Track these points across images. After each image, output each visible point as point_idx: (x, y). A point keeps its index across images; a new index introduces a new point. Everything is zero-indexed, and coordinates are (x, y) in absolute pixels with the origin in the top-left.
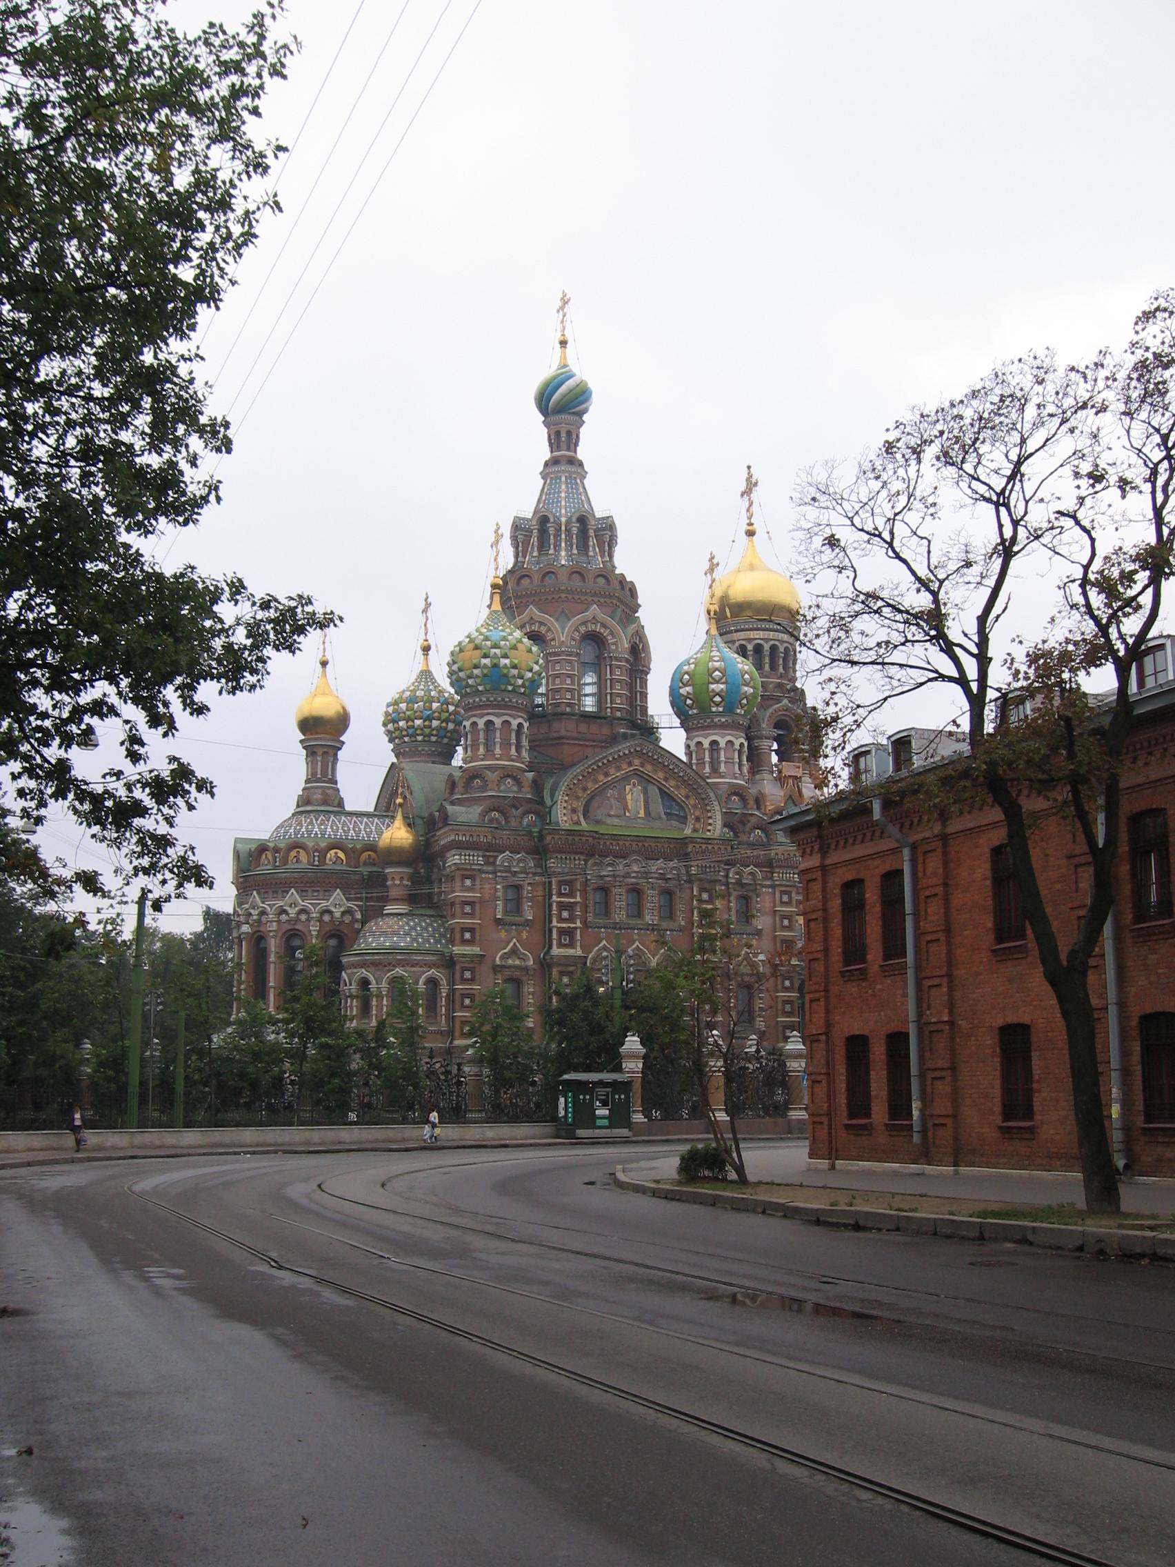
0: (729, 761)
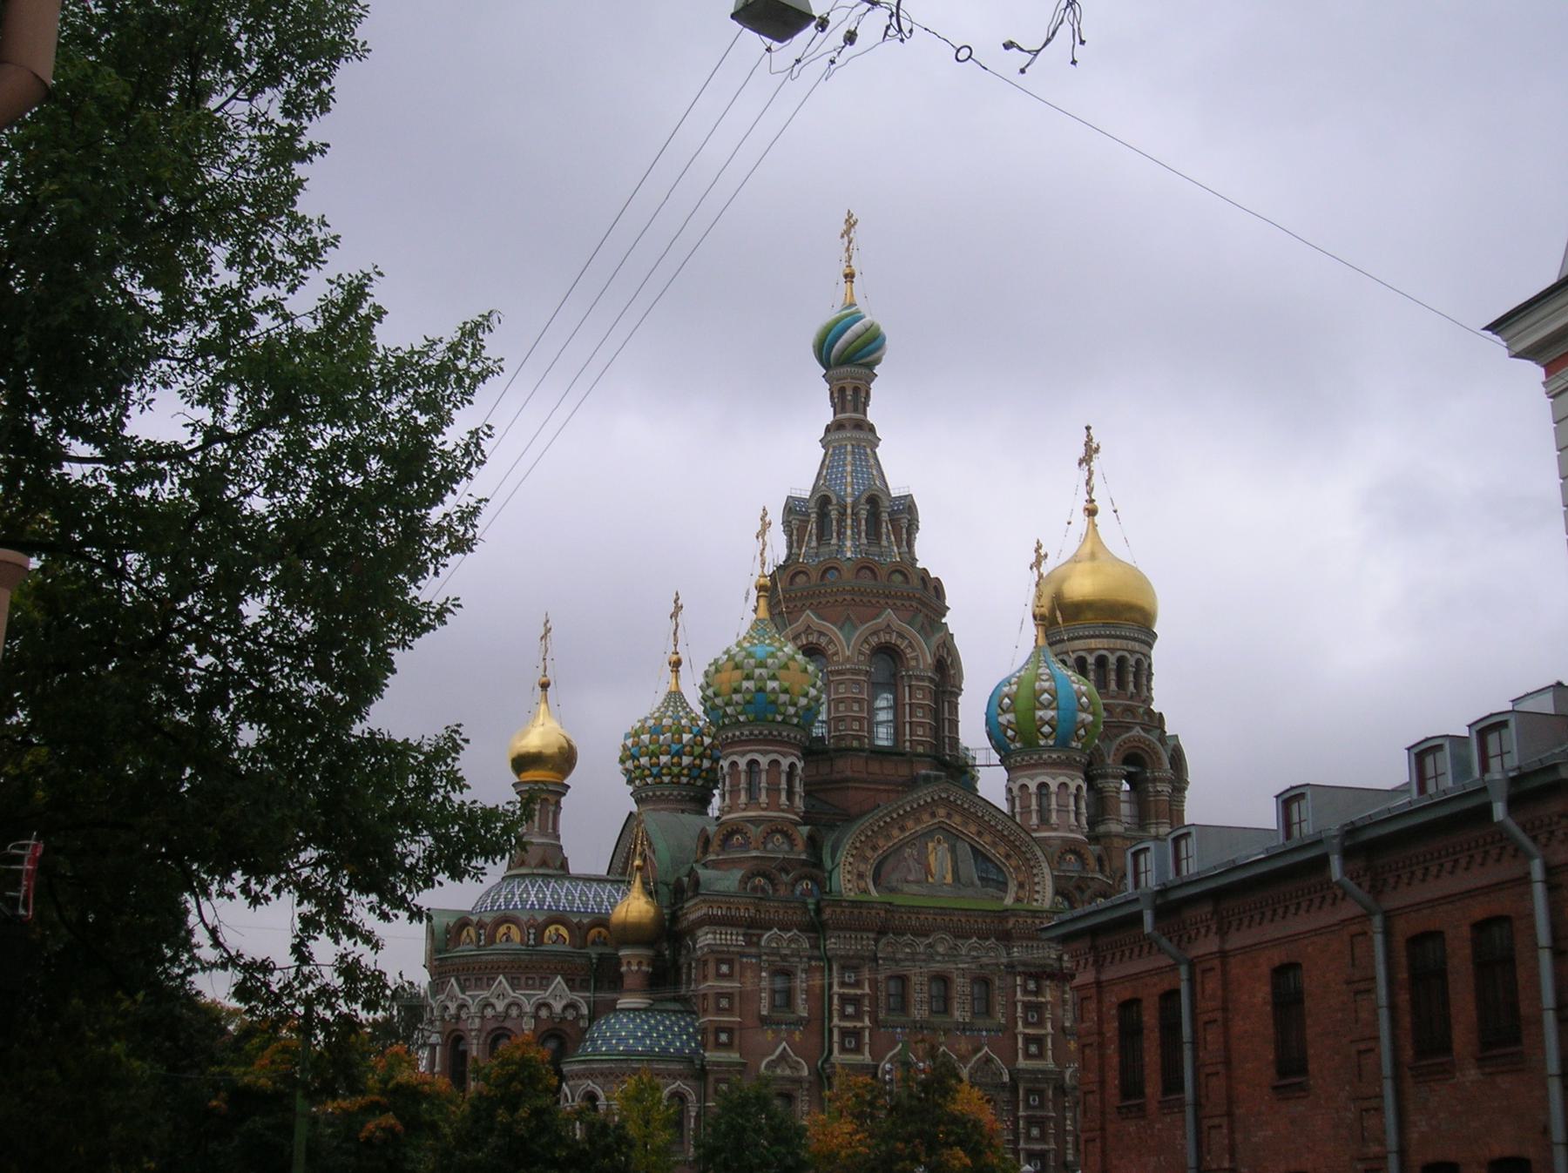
0: (1063, 809)
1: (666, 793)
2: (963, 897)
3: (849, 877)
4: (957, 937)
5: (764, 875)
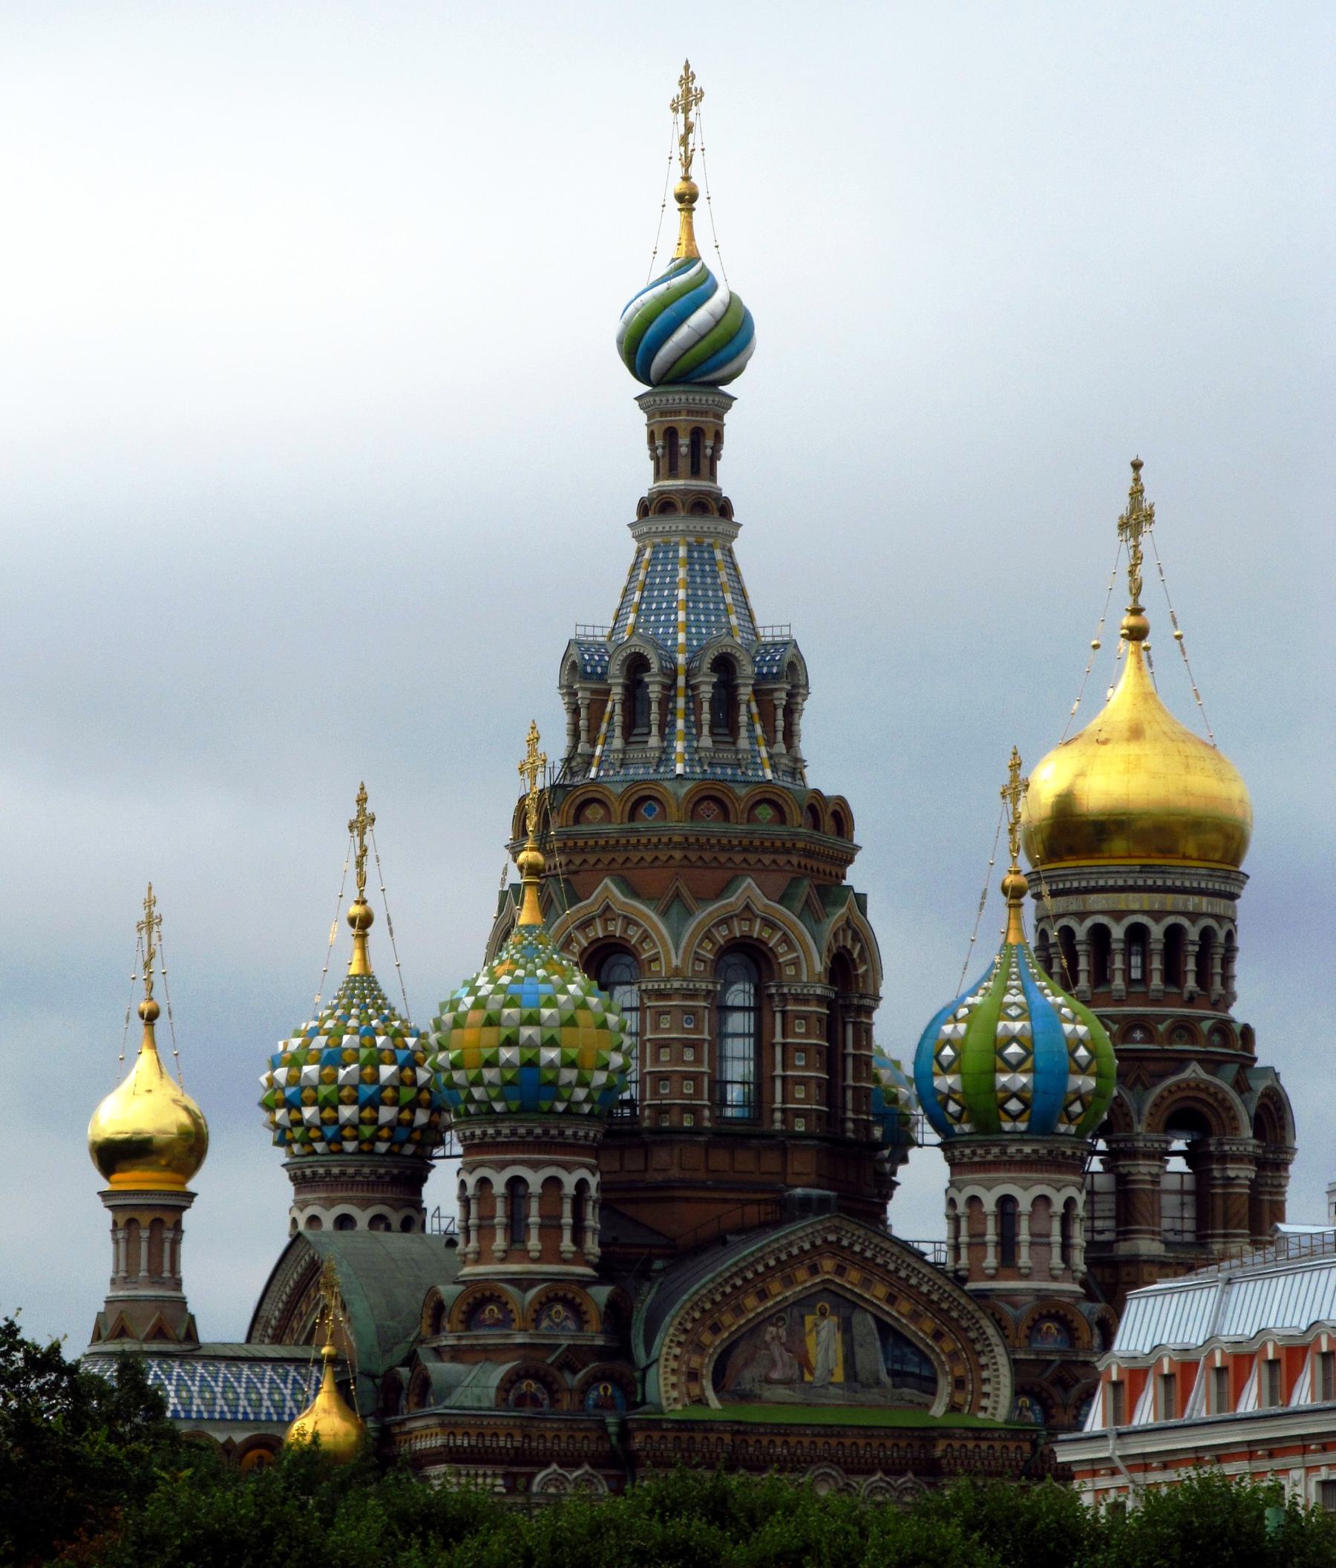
0: (1040, 1240)
1: (351, 1171)
2: (862, 1405)
3: (673, 1379)
4: (849, 1472)
5: (536, 1376)
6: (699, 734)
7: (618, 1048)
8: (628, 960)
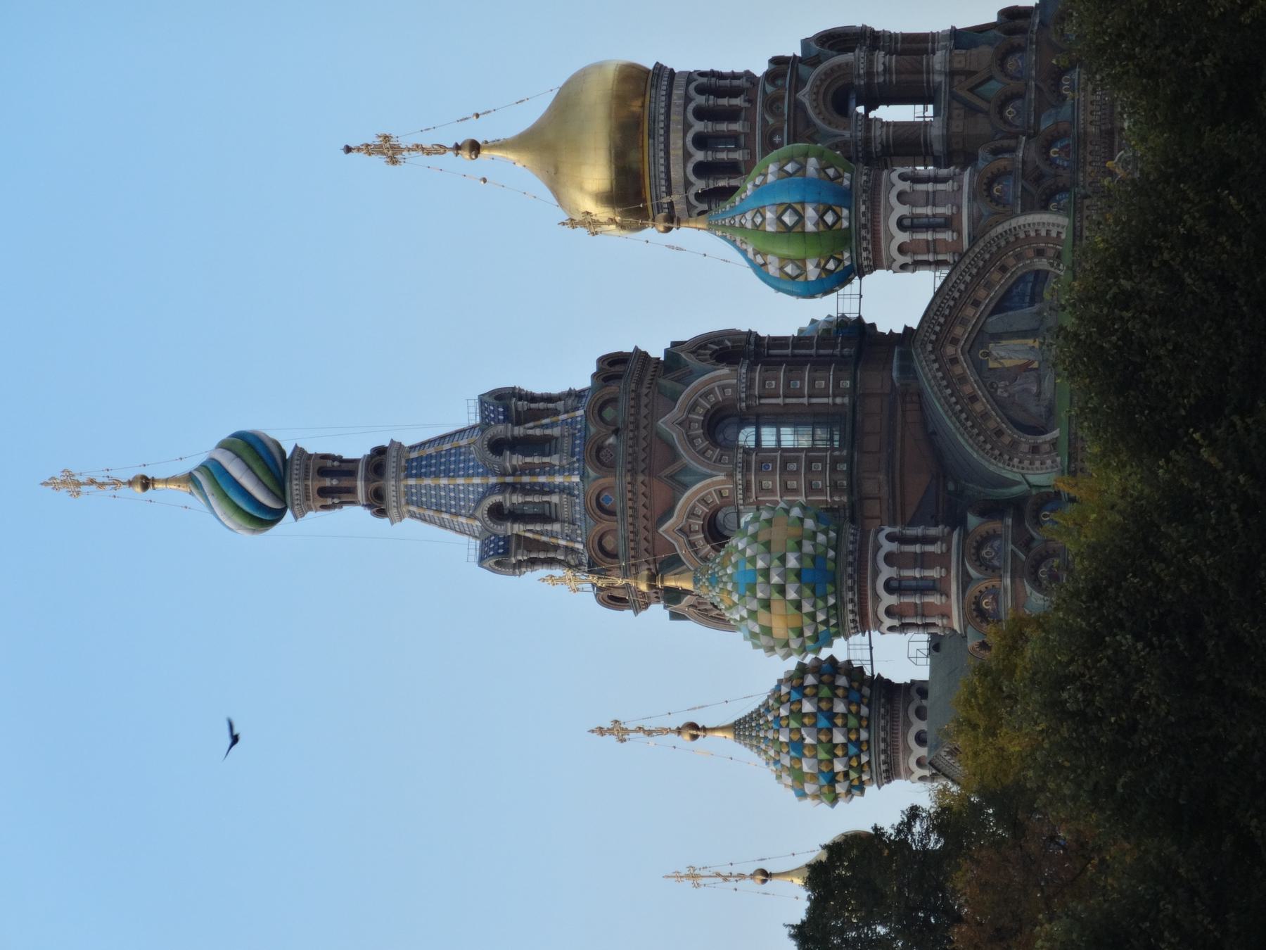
0: (931, 199)
1: (882, 734)
3: (1038, 463)
6: (550, 464)
7: (787, 511)
8: (720, 515)
